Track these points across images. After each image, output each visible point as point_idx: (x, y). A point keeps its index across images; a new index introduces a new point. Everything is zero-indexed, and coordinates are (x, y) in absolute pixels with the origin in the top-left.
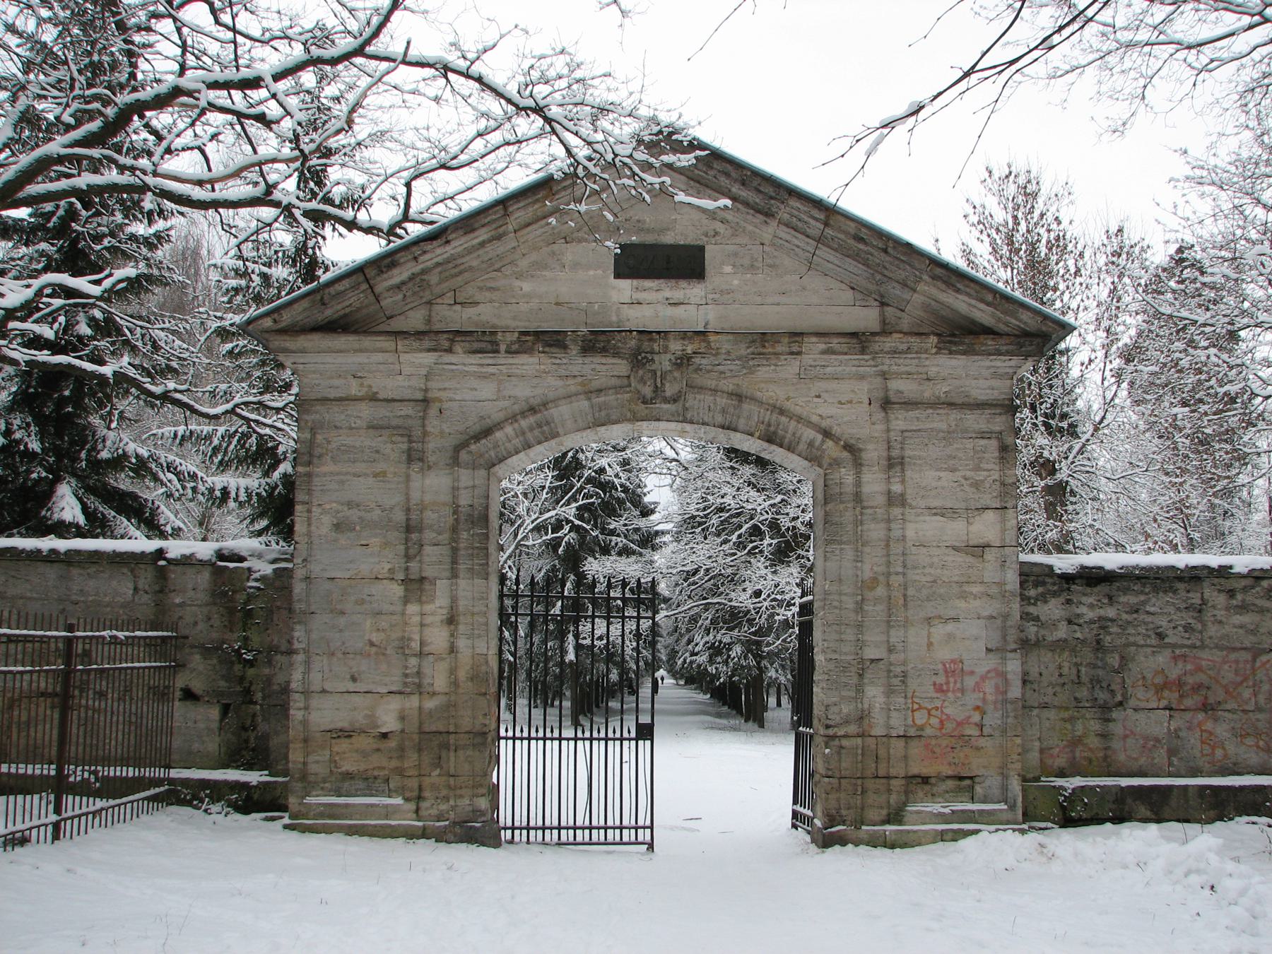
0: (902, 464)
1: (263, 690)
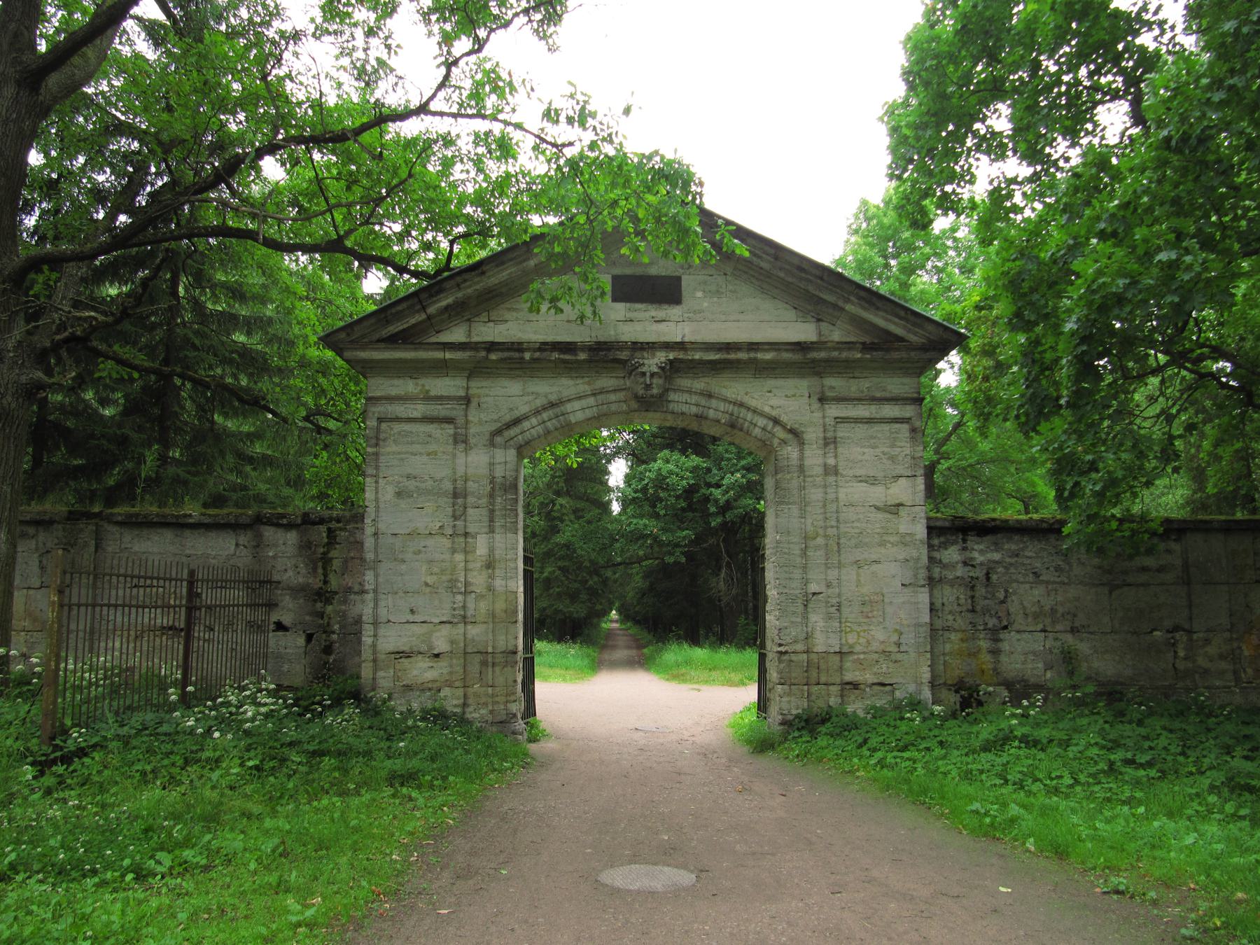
0: (835, 442)
1: (339, 623)
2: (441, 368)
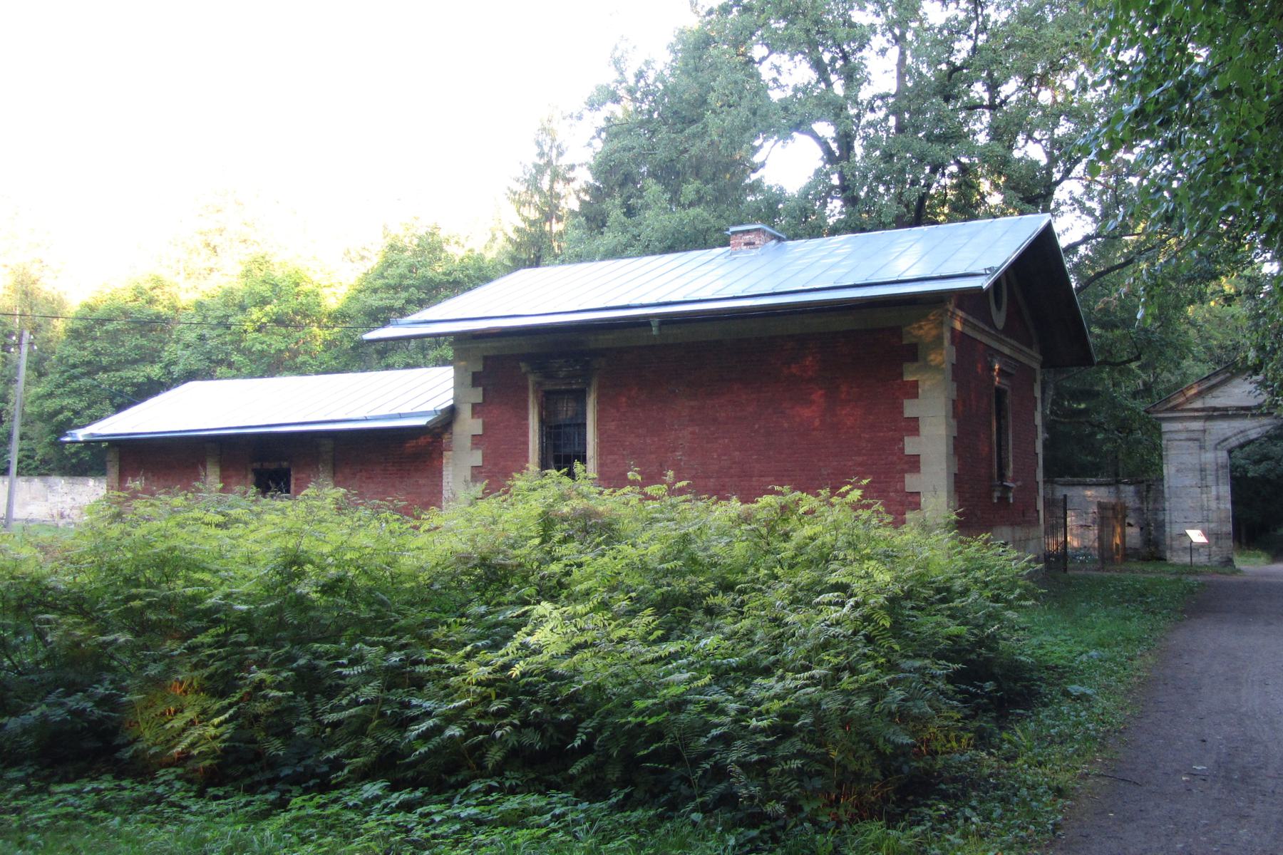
2: (1195, 418)
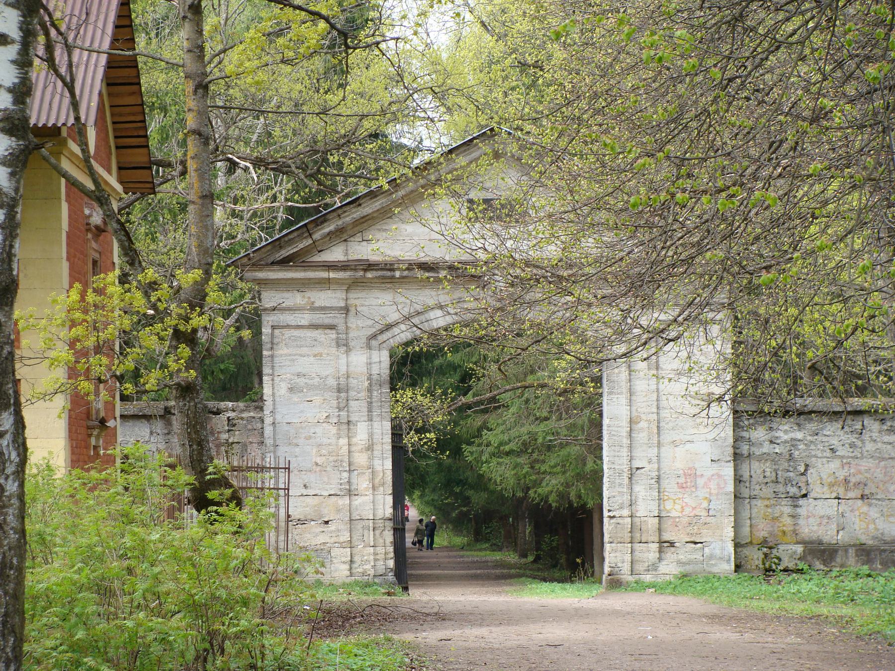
2: (325, 284)
